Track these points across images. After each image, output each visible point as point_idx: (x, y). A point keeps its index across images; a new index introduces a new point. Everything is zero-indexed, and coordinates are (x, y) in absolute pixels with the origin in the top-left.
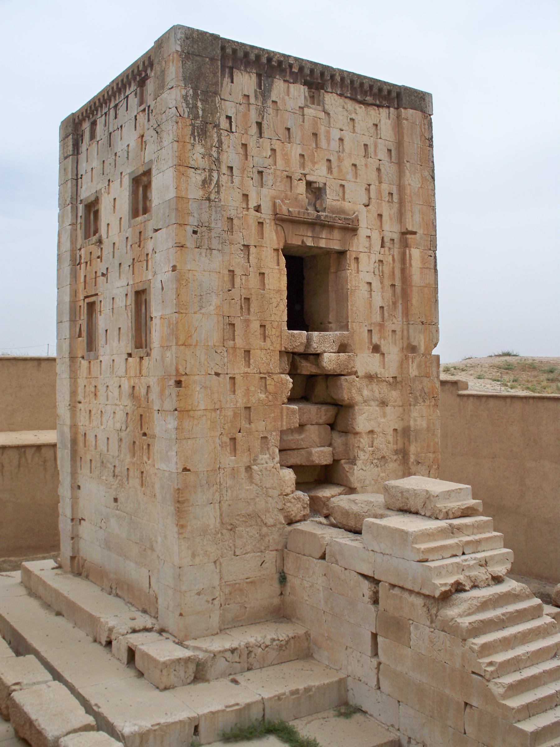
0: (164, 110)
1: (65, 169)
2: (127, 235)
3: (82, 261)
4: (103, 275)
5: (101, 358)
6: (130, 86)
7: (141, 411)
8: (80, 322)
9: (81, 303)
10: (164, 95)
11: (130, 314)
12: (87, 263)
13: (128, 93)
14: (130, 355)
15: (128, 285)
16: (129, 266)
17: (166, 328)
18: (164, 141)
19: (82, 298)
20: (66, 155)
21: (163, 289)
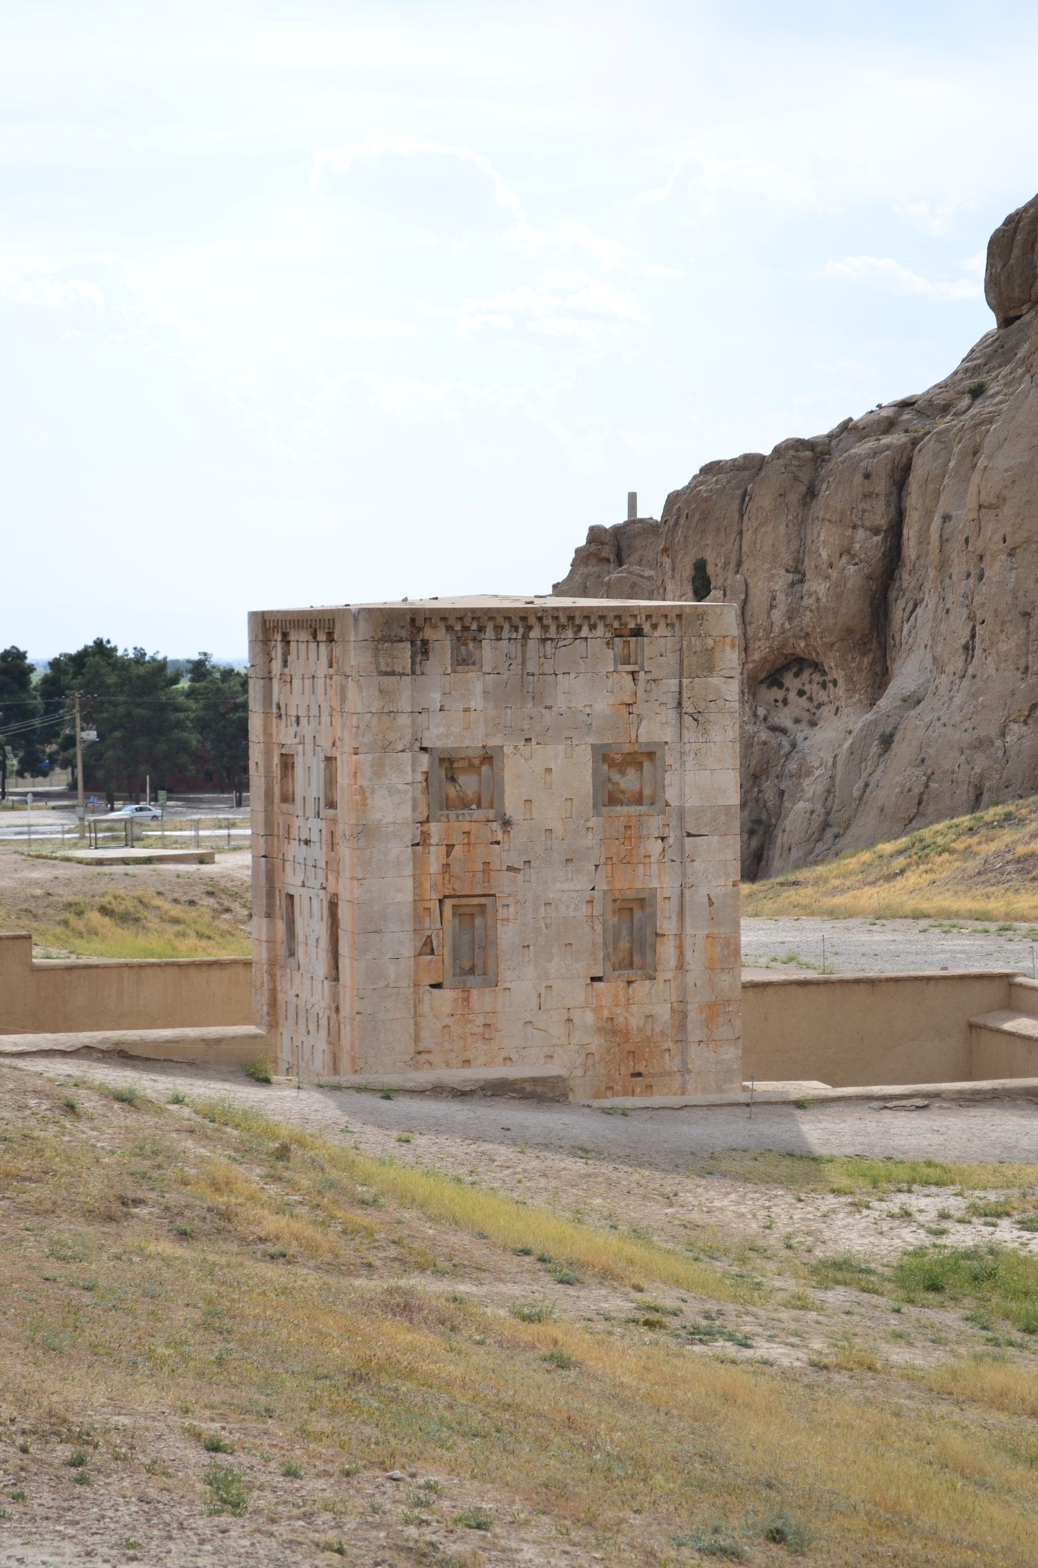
0: (711, 697)
1: (381, 692)
2: (590, 824)
3: (434, 840)
4: (510, 869)
5: (508, 985)
6: (593, 627)
7: (629, 1047)
8: (428, 933)
9: (435, 905)
10: (715, 681)
11: (599, 928)
12: (450, 847)
13: (585, 632)
14: (599, 979)
15: (593, 889)
16: (597, 866)
17: (719, 949)
18: (713, 734)
19: (435, 896)
20: (384, 669)
21: (711, 903)
